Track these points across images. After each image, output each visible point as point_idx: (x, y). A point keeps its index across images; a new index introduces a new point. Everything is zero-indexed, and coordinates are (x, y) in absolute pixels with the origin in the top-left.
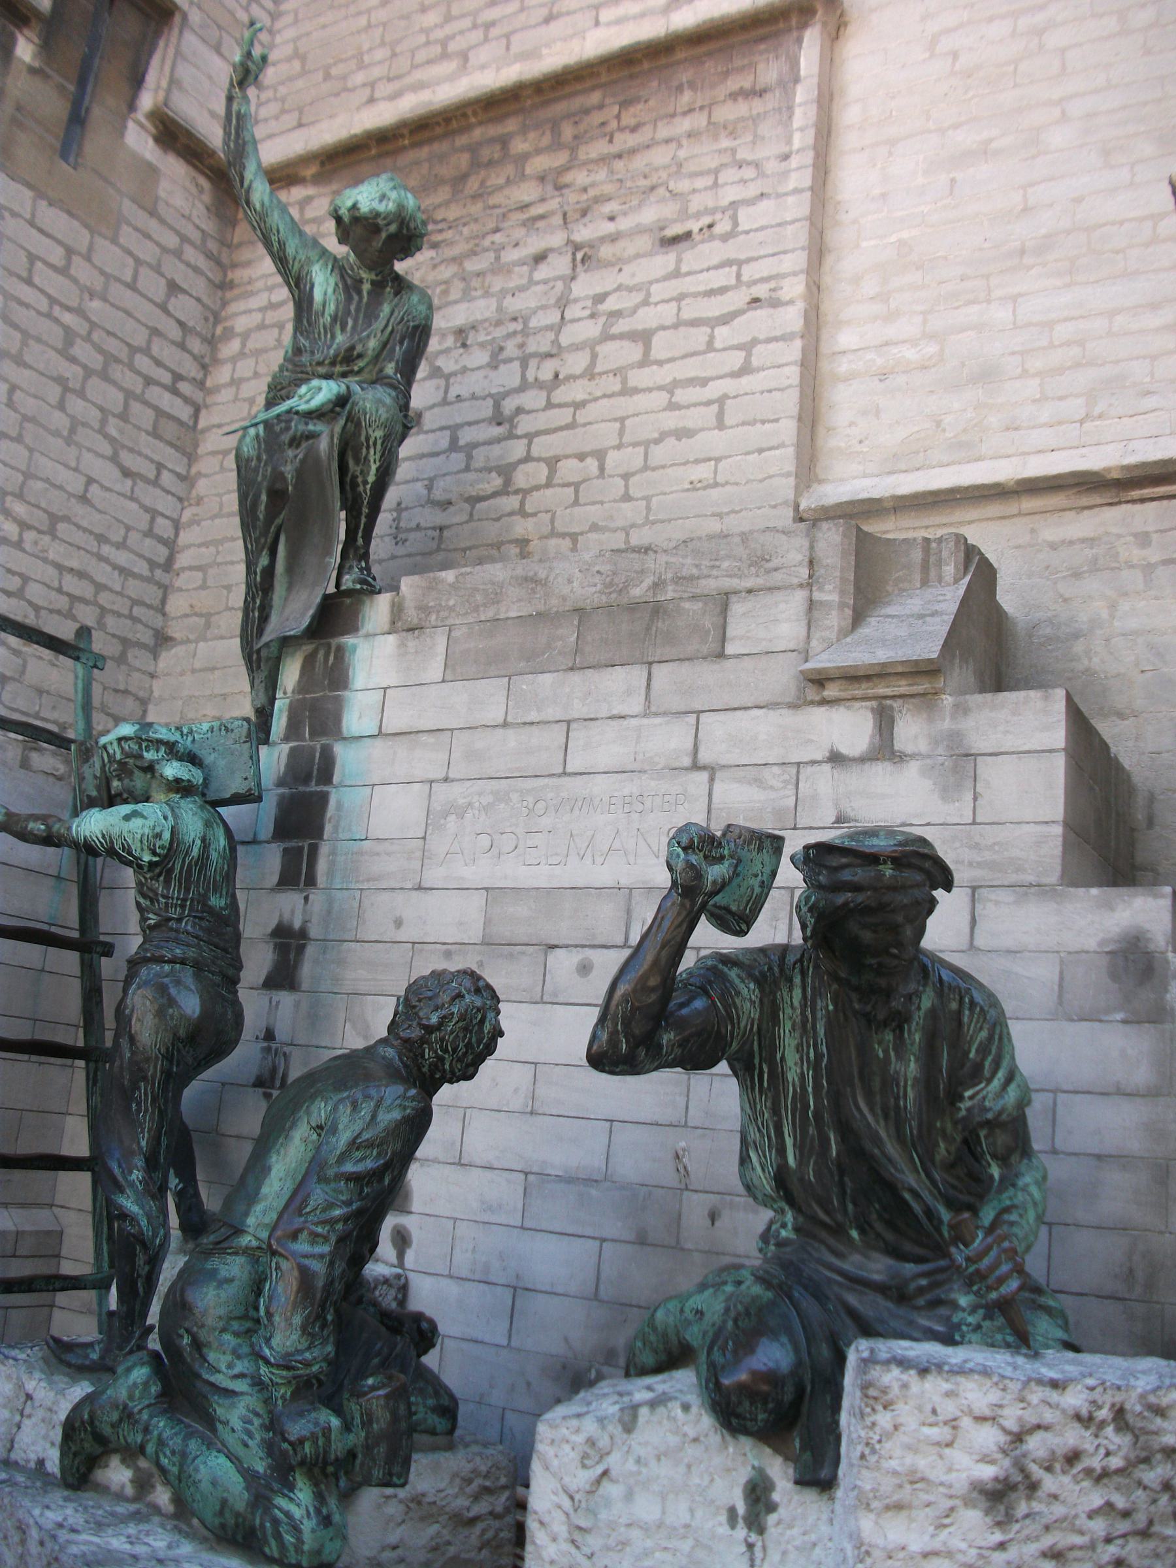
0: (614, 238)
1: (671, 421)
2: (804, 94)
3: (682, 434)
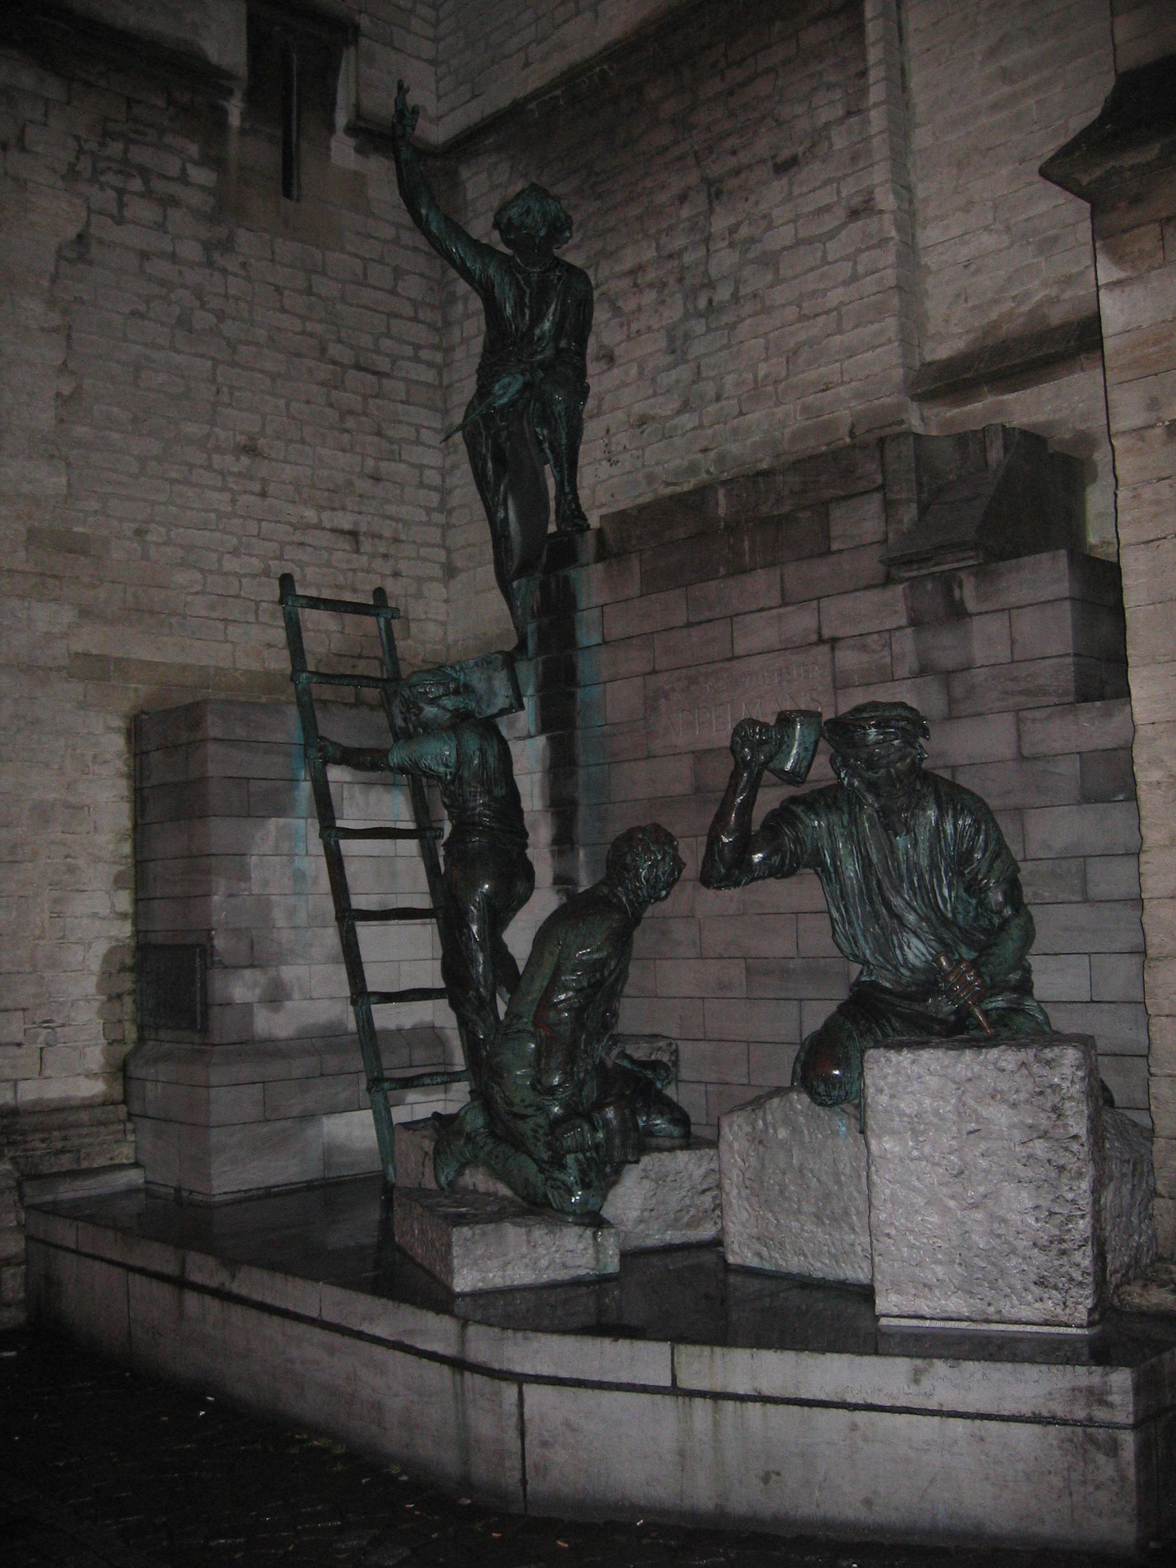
0: (737, 172)
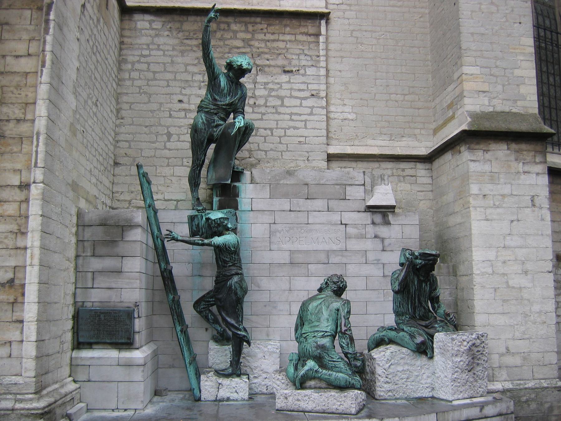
0: (269, 66)
1: (291, 124)
2: (322, 39)
3: (295, 128)
